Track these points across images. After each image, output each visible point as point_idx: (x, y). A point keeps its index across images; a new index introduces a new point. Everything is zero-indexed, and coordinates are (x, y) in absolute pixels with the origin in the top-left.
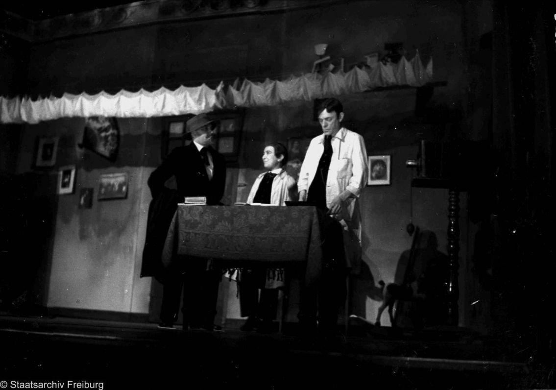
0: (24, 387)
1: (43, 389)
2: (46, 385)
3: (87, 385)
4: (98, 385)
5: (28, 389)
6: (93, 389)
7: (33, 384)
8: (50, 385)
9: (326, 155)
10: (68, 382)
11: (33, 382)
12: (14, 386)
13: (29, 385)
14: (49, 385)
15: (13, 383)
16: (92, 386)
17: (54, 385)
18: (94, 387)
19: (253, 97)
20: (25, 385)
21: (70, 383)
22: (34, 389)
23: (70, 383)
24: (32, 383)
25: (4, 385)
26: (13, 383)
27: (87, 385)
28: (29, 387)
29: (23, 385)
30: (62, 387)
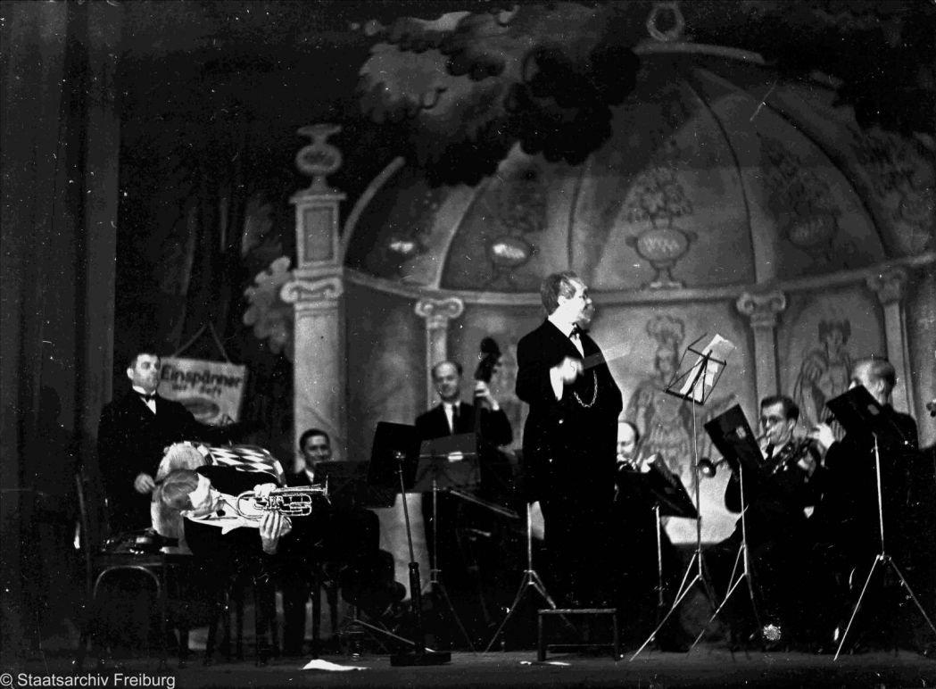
2: (78, 680)
3: (147, 681)
4: (165, 680)
7: (55, 680)
8: (84, 681)
10: (116, 675)
11: (56, 676)
12: (24, 682)
13: (49, 681)
14: (84, 681)
16: (156, 682)
17: (92, 680)
18: (159, 684)
19: (423, 259)
21: (118, 677)
23: (118, 677)
24: (53, 677)
25: (6, 680)
27: (147, 681)
28: (49, 684)
29: (39, 682)
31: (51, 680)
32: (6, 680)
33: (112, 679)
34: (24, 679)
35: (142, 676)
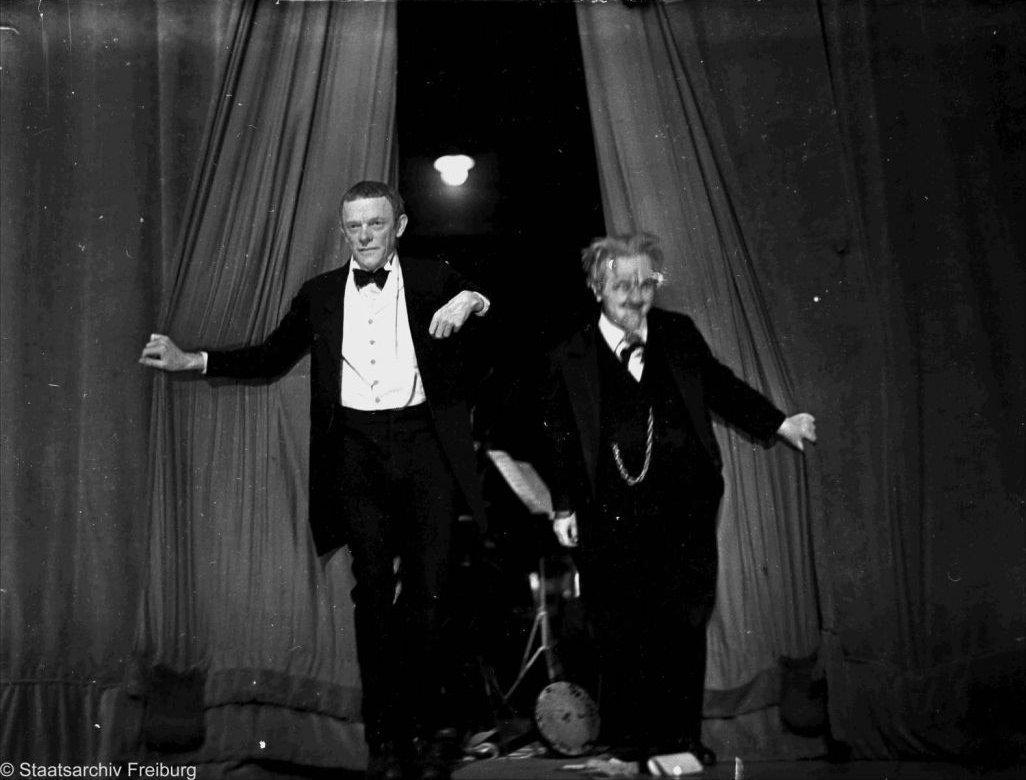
0: (45, 775)
1: (82, 778)
2: (87, 771)
3: (165, 771)
4: (185, 770)
5: (54, 778)
6: (176, 778)
8: (94, 771)
9: (454, 312)
15: (24, 766)
16: (175, 773)
18: (178, 774)
20: (47, 771)
21: (132, 766)
22: (64, 778)
23: (132, 766)
25: (7, 770)
26: (25, 766)
27: (165, 771)
28: (55, 774)
29: (43, 771)
30: (117, 775)
31: (58, 770)
32: (7, 770)
33: (125, 770)
34: (28, 769)
35: (159, 766)
